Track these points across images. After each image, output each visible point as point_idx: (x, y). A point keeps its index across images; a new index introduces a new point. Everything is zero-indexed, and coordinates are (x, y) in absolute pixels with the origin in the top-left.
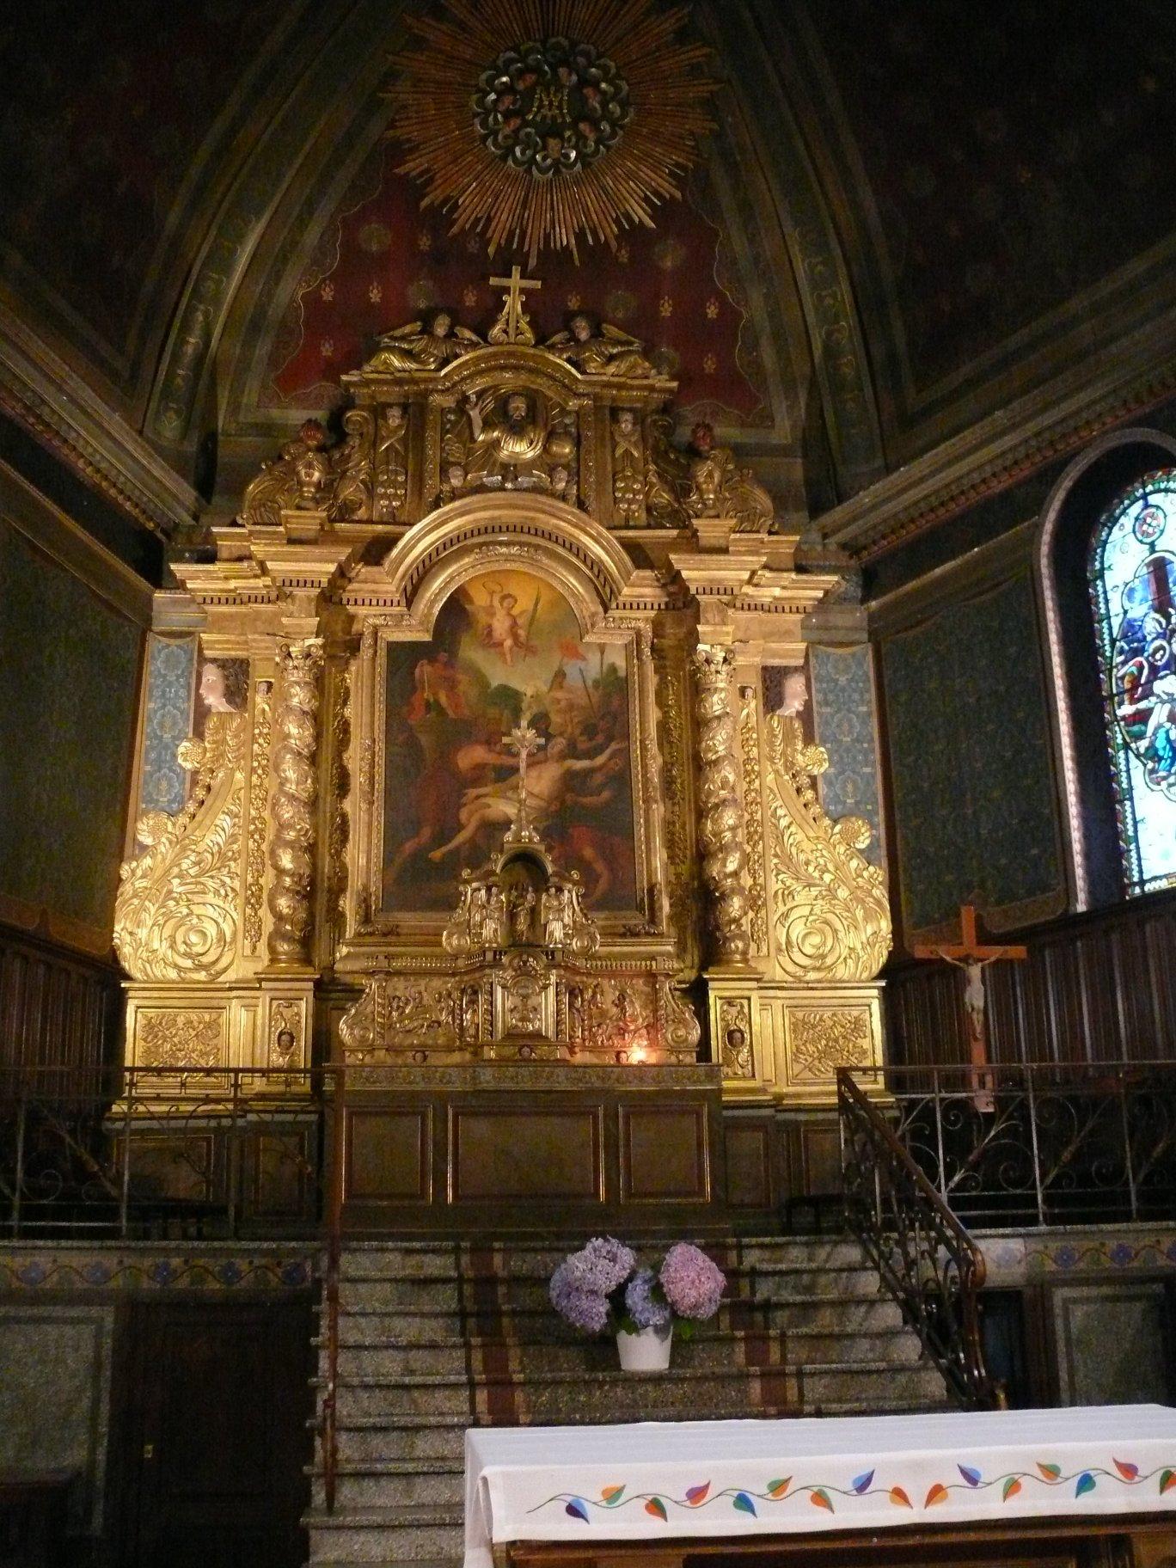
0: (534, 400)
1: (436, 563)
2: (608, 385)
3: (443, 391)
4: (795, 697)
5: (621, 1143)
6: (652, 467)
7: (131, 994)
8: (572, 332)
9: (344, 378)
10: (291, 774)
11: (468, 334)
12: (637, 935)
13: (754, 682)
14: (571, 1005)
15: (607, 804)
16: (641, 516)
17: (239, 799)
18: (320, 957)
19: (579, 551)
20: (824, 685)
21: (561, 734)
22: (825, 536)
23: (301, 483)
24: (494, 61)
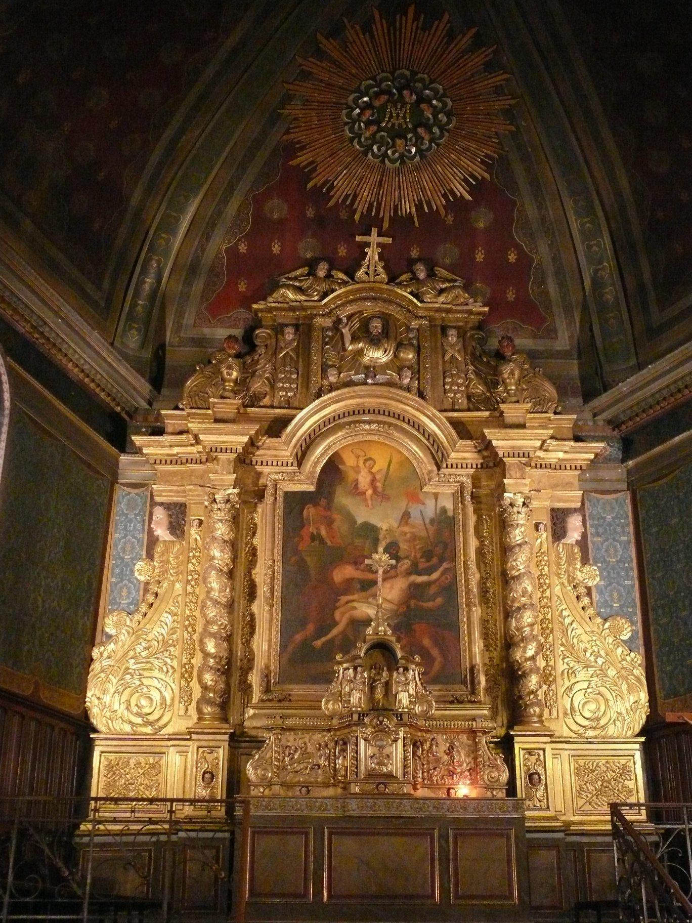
0: (386, 319)
1: (319, 436)
2: (438, 310)
3: (323, 315)
4: (575, 529)
5: (451, 857)
6: (471, 368)
7: (97, 742)
8: (414, 273)
9: (255, 306)
10: (215, 585)
11: (341, 275)
12: (461, 702)
13: (545, 519)
14: (414, 753)
15: (439, 608)
16: (463, 402)
17: (178, 602)
18: (234, 717)
19: (420, 427)
20: (596, 522)
21: (407, 557)
22: (595, 415)
23: (223, 380)
24: (359, 87)
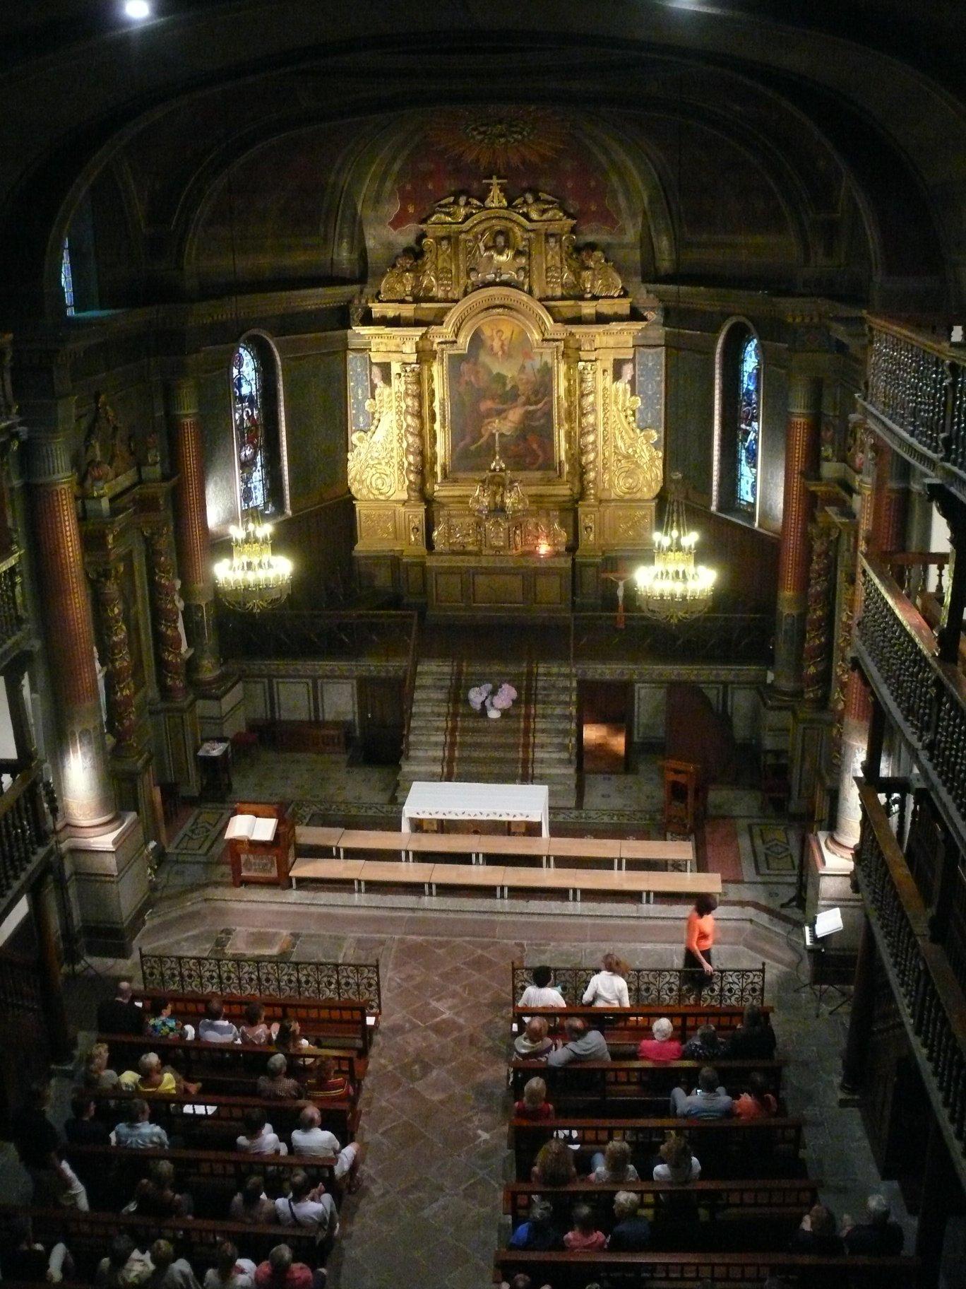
11: (475, 202)
13: (609, 365)
15: (543, 425)
